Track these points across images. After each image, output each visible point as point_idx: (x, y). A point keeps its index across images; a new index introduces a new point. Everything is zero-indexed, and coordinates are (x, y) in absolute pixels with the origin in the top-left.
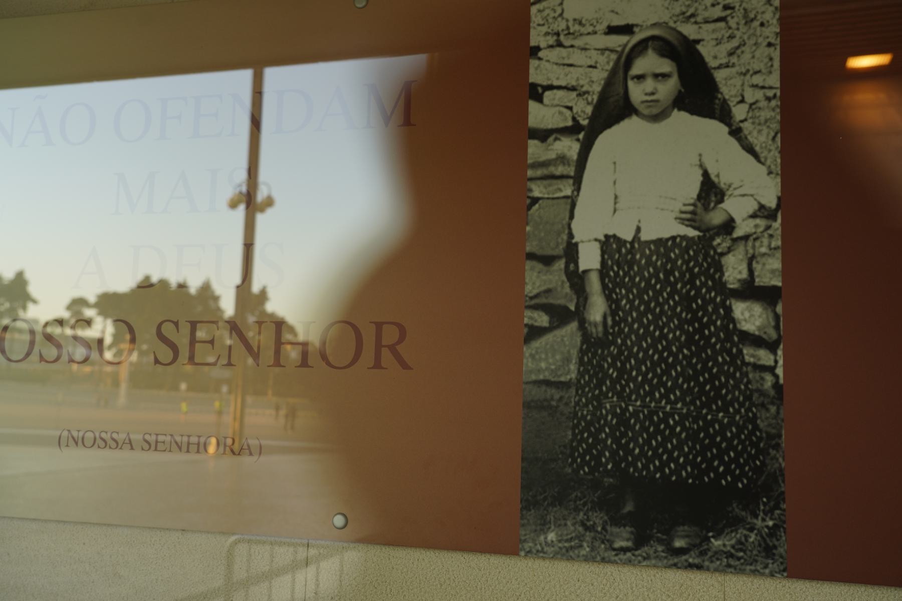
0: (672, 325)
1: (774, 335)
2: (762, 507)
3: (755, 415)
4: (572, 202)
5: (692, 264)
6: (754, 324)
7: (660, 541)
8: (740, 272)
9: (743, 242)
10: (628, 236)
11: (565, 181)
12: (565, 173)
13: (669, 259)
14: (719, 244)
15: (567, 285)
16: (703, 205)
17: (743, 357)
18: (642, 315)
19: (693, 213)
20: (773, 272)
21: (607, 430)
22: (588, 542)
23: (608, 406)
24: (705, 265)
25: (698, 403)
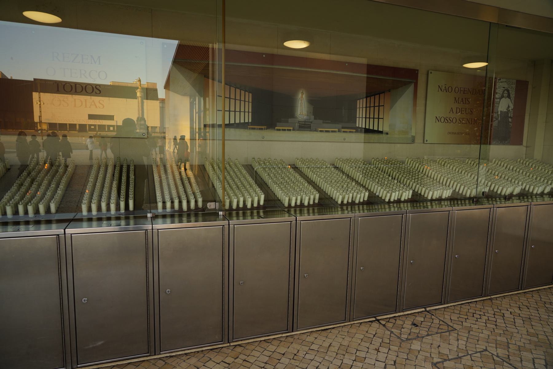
4: (498, 106)
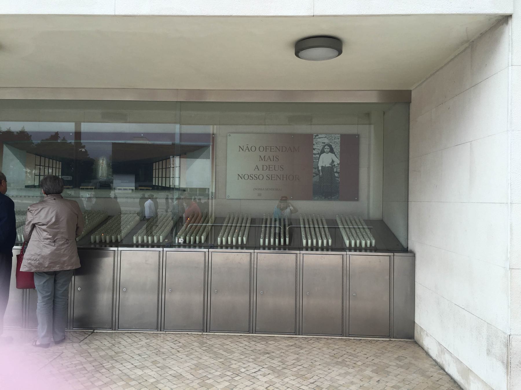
1: (338, 177)
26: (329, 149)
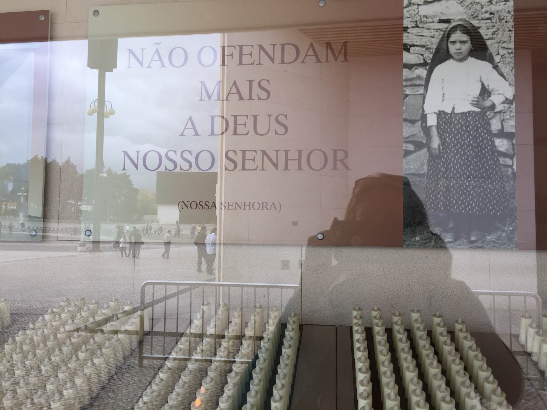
0: (469, 149)
1: (512, 152)
2: (507, 222)
3: (504, 185)
4: (424, 96)
5: (477, 123)
6: (504, 148)
7: (465, 238)
8: (498, 126)
9: (499, 114)
10: (449, 111)
11: (420, 87)
12: (420, 83)
13: (467, 121)
14: (489, 115)
15: (422, 132)
16: (482, 98)
17: (499, 162)
18: (455, 145)
19: (477, 101)
20: (512, 126)
21: (441, 193)
22: (434, 240)
23: (441, 183)
24: (483, 123)
25: (480, 181)
26: (469, 43)
